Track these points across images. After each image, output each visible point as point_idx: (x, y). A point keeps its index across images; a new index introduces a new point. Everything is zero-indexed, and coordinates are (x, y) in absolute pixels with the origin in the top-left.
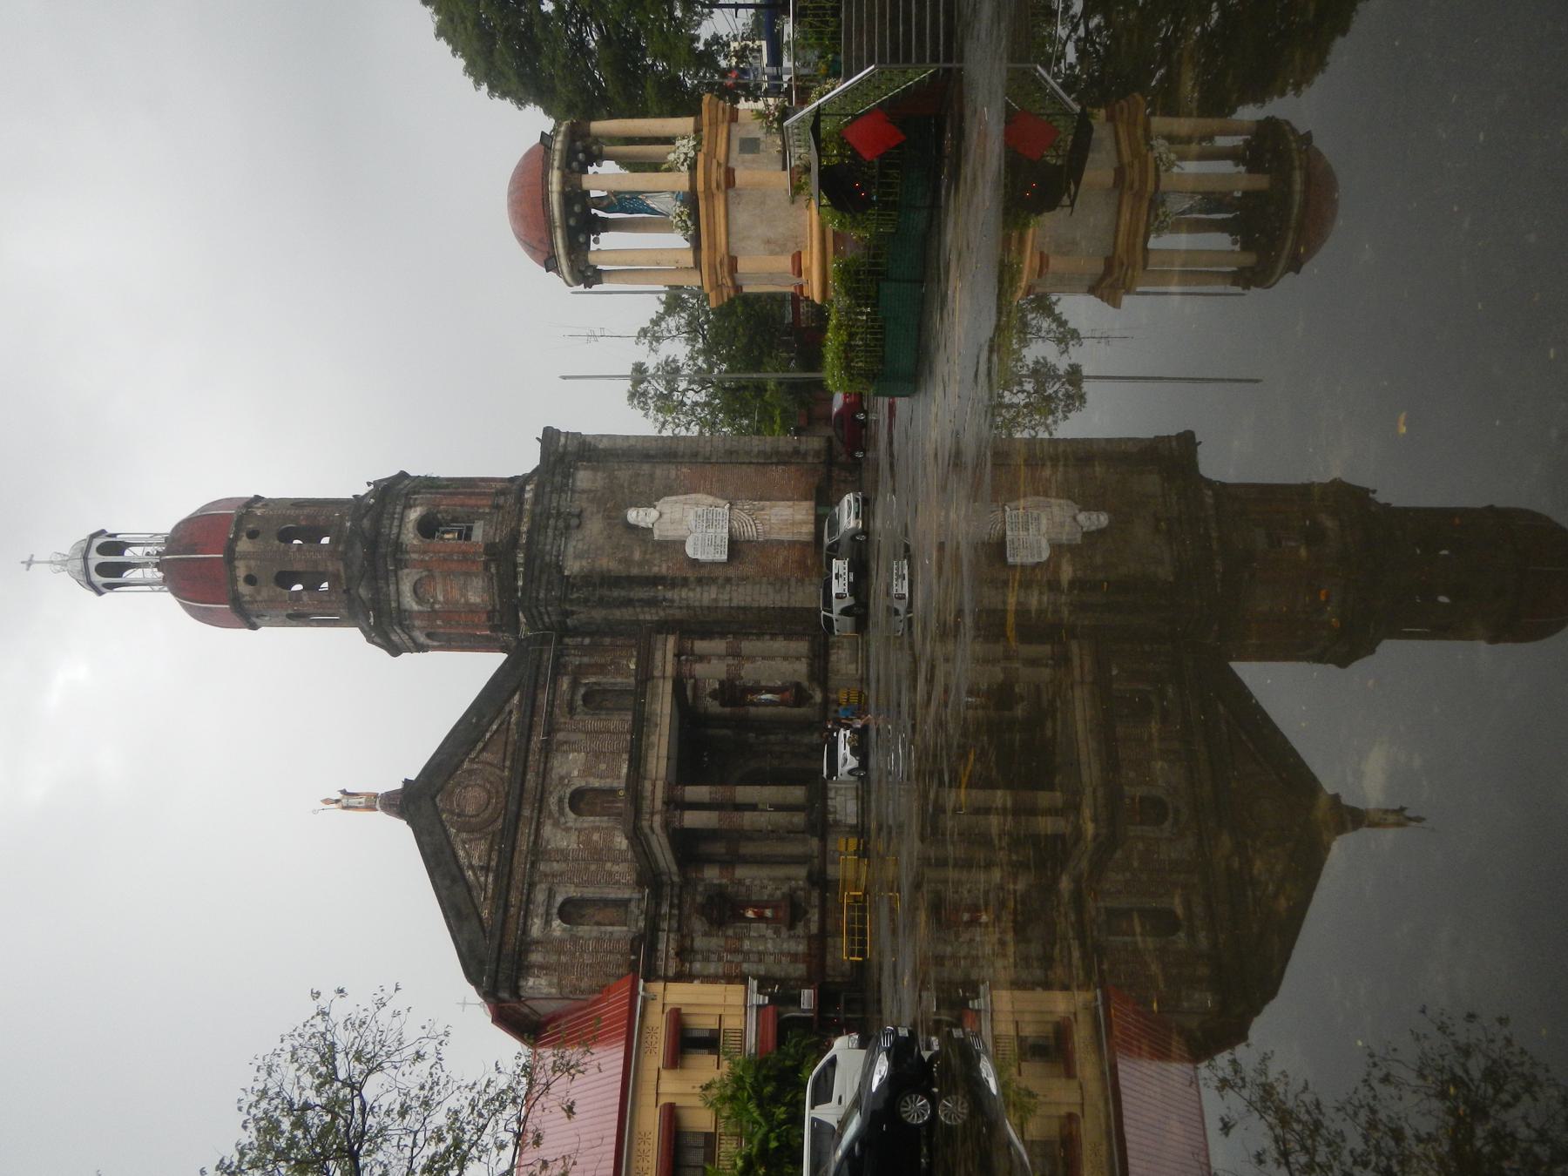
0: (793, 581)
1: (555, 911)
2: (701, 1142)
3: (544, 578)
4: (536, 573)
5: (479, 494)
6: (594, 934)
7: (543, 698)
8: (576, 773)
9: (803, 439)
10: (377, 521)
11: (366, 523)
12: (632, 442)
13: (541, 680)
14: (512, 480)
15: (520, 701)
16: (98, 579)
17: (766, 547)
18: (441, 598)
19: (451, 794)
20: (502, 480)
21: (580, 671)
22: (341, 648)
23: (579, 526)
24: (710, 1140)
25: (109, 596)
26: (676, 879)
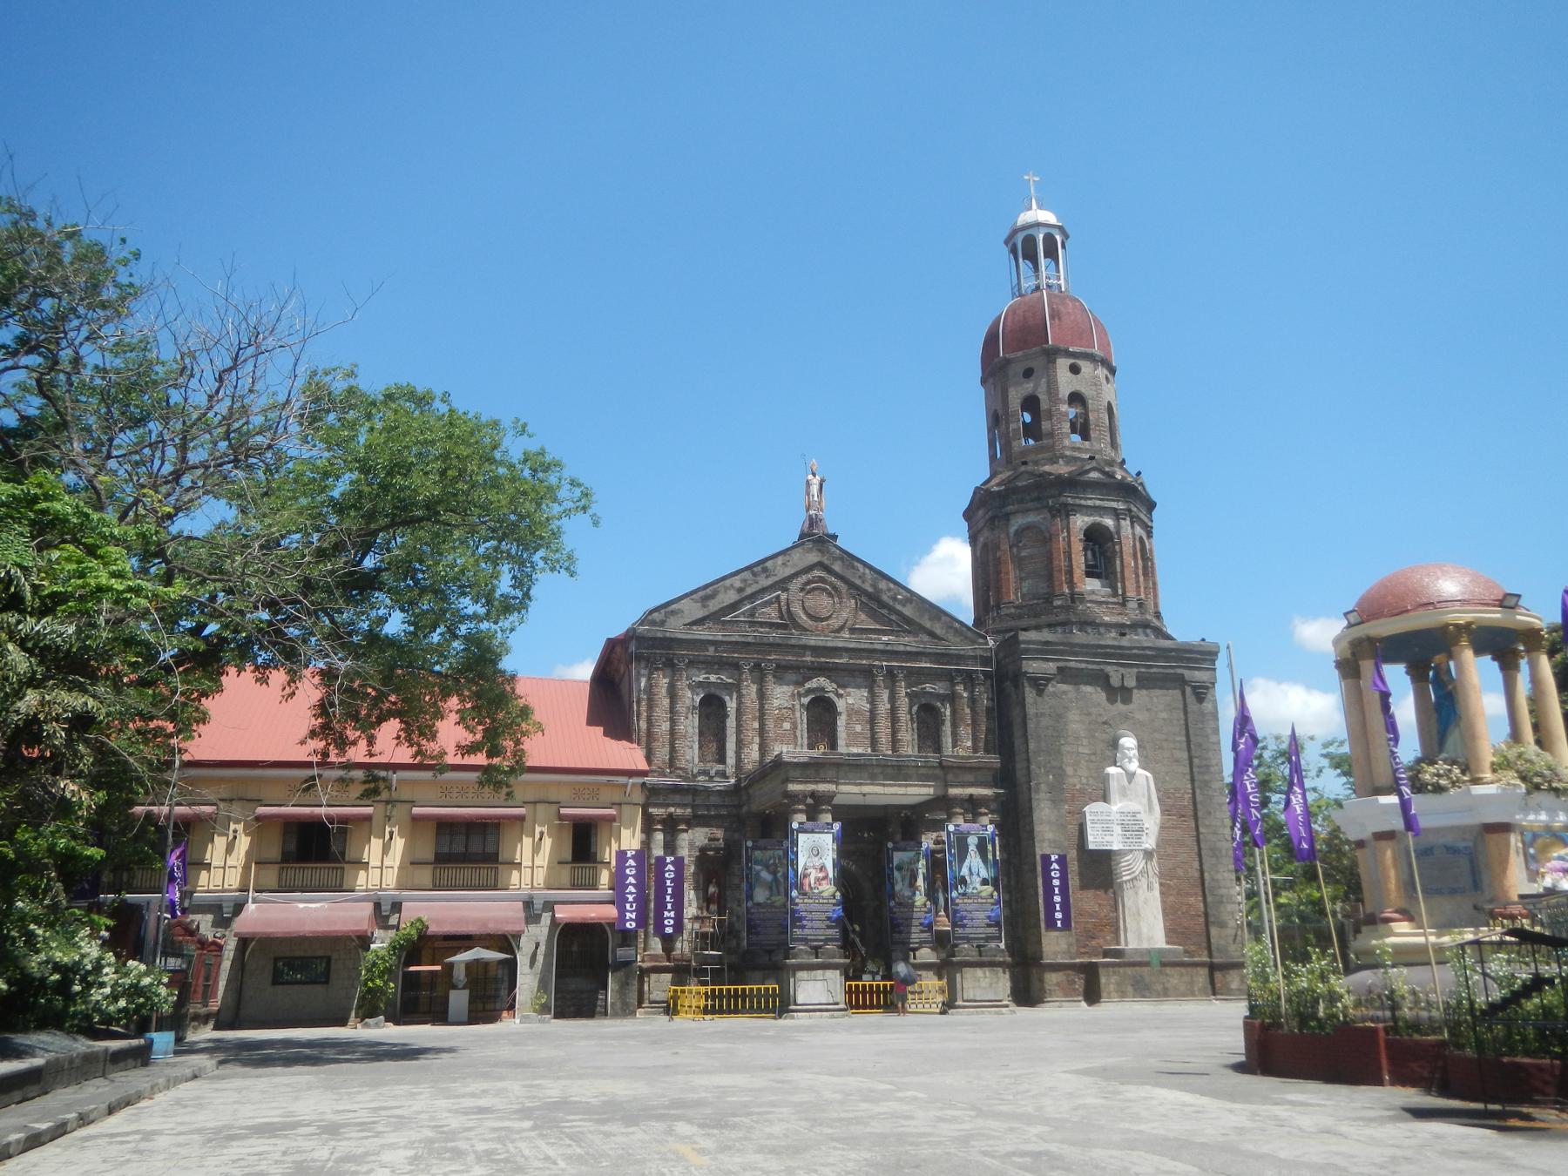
1: (713, 690)
2: (490, 849)
5: (1138, 582)
6: (690, 730)
8: (850, 701)
10: (1094, 486)
11: (1094, 475)
12: (1213, 739)
14: (1158, 615)
18: (1023, 554)
20: (1156, 605)
21: (952, 698)
22: (970, 465)
25: (1006, 250)
26: (745, 809)
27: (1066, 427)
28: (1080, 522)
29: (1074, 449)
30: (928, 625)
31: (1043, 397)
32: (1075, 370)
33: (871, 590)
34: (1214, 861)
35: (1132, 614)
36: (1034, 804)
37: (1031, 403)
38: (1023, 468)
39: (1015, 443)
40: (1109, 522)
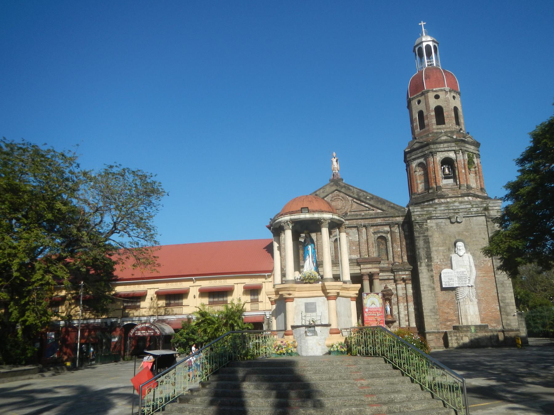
0: (438, 317)
3: (425, 213)
4: (425, 209)
7: (379, 221)
8: (350, 238)
9: (516, 317)
11: (444, 138)
13: (387, 219)
15: (378, 213)
16: (417, 49)
17: (456, 304)
19: (339, 196)
21: (392, 233)
23: (452, 223)
24: (226, 302)
25: (414, 54)
27: (434, 121)
28: (439, 157)
29: (438, 129)
30: (380, 207)
31: (424, 111)
32: (437, 97)
33: (356, 197)
34: (503, 289)
35: (464, 190)
36: (420, 271)
37: (421, 113)
38: (416, 141)
39: (416, 131)
40: (452, 155)
